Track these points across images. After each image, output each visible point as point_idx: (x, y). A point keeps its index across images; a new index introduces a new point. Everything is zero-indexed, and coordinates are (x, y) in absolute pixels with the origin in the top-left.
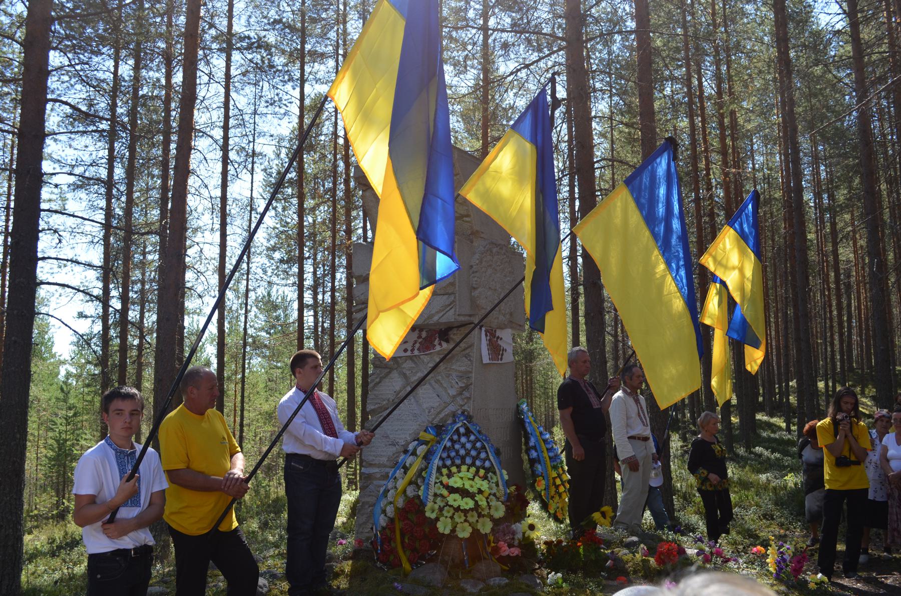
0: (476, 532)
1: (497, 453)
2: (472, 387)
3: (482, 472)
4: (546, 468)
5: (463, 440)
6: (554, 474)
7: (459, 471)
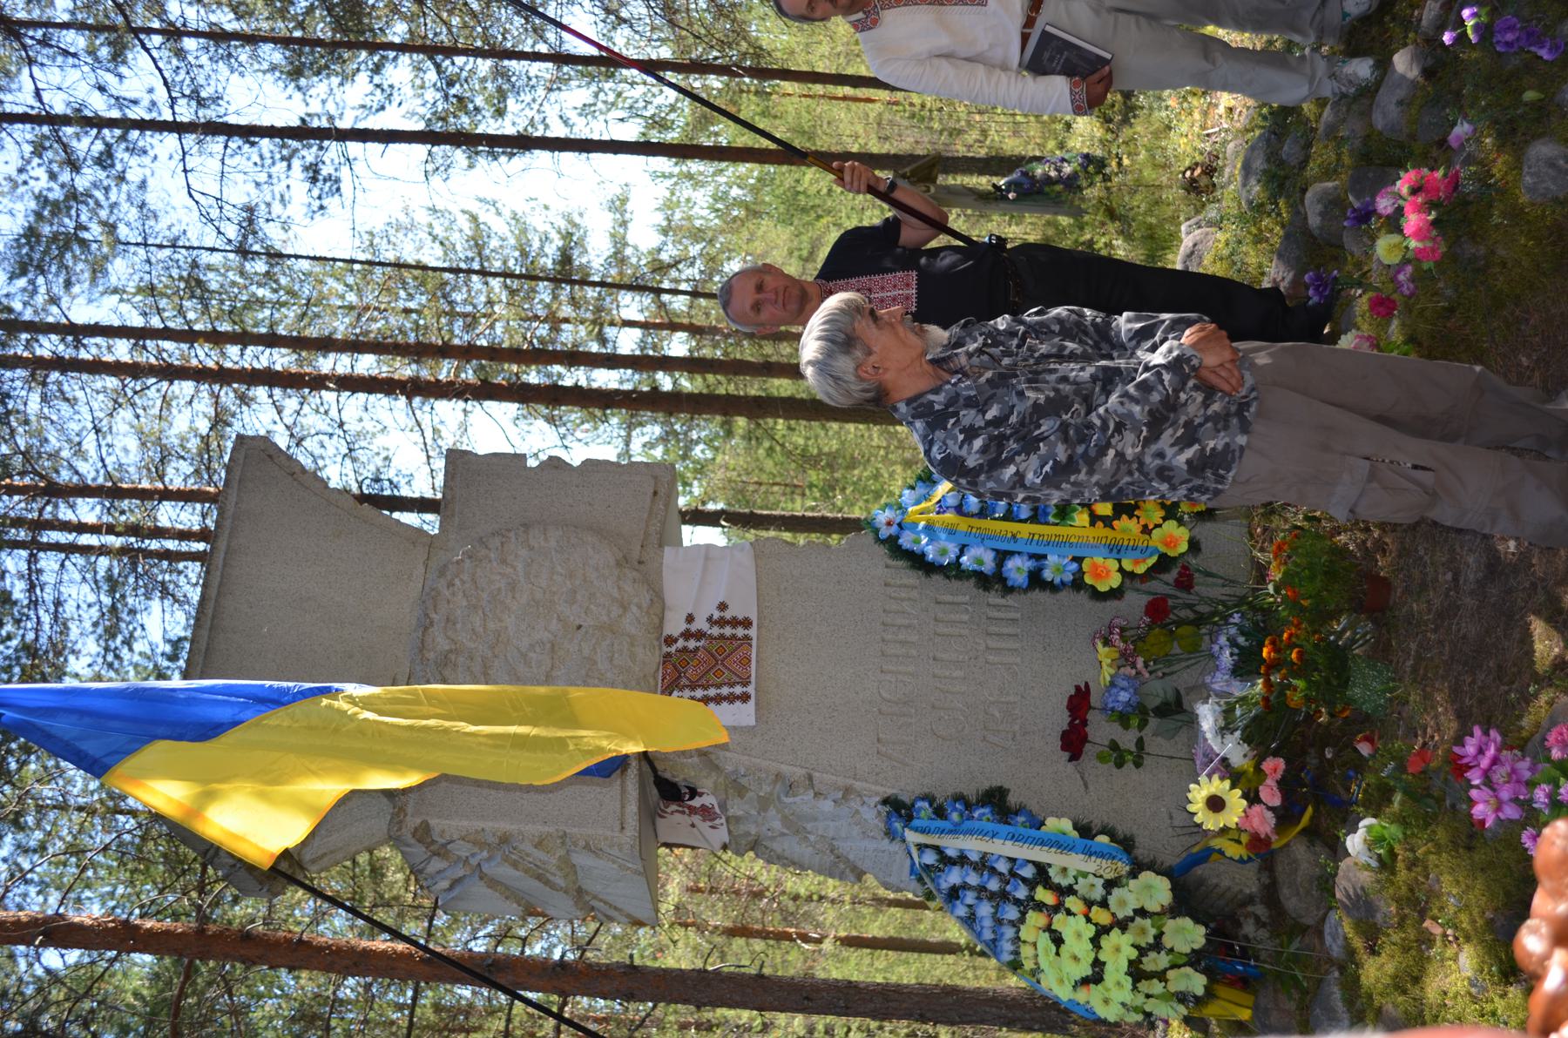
0: (1195, 959)
1: (998, 803)
2: (816, 775)
3: (1044, 895)
4: (1060, 544)
5: (954, 877)
7: (1035, 945)
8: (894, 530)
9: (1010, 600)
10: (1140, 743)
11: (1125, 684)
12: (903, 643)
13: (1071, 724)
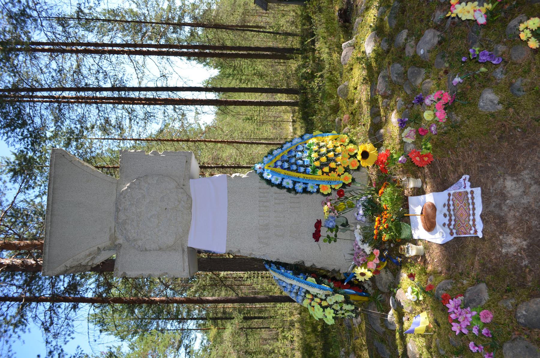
6: (319, 172)
8: (261, 170)
9: (298, 195)
10: (336, 236)
11: (331, 219)
12: (265, 207)
13: (316, 231)
